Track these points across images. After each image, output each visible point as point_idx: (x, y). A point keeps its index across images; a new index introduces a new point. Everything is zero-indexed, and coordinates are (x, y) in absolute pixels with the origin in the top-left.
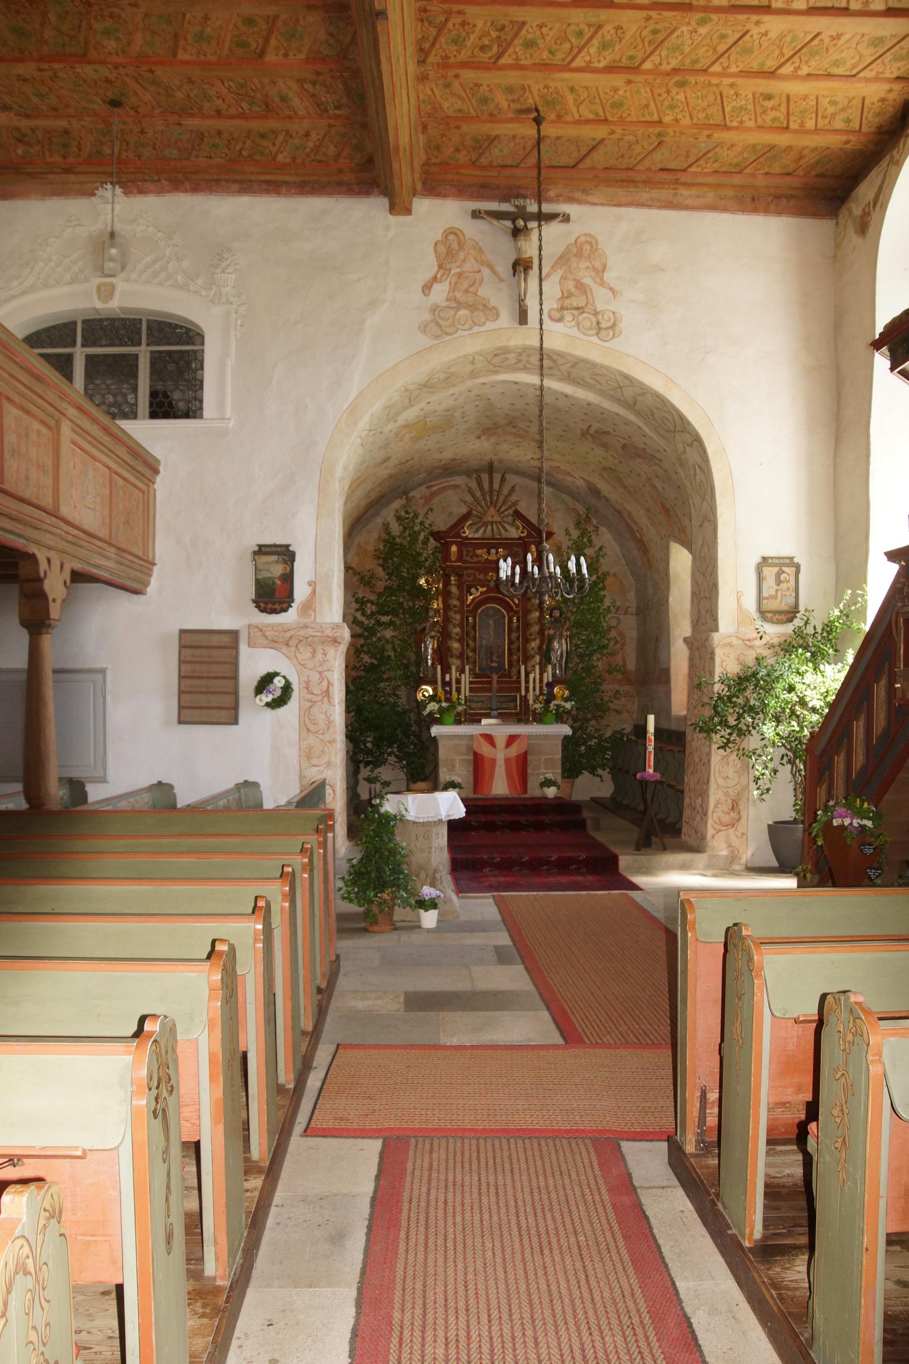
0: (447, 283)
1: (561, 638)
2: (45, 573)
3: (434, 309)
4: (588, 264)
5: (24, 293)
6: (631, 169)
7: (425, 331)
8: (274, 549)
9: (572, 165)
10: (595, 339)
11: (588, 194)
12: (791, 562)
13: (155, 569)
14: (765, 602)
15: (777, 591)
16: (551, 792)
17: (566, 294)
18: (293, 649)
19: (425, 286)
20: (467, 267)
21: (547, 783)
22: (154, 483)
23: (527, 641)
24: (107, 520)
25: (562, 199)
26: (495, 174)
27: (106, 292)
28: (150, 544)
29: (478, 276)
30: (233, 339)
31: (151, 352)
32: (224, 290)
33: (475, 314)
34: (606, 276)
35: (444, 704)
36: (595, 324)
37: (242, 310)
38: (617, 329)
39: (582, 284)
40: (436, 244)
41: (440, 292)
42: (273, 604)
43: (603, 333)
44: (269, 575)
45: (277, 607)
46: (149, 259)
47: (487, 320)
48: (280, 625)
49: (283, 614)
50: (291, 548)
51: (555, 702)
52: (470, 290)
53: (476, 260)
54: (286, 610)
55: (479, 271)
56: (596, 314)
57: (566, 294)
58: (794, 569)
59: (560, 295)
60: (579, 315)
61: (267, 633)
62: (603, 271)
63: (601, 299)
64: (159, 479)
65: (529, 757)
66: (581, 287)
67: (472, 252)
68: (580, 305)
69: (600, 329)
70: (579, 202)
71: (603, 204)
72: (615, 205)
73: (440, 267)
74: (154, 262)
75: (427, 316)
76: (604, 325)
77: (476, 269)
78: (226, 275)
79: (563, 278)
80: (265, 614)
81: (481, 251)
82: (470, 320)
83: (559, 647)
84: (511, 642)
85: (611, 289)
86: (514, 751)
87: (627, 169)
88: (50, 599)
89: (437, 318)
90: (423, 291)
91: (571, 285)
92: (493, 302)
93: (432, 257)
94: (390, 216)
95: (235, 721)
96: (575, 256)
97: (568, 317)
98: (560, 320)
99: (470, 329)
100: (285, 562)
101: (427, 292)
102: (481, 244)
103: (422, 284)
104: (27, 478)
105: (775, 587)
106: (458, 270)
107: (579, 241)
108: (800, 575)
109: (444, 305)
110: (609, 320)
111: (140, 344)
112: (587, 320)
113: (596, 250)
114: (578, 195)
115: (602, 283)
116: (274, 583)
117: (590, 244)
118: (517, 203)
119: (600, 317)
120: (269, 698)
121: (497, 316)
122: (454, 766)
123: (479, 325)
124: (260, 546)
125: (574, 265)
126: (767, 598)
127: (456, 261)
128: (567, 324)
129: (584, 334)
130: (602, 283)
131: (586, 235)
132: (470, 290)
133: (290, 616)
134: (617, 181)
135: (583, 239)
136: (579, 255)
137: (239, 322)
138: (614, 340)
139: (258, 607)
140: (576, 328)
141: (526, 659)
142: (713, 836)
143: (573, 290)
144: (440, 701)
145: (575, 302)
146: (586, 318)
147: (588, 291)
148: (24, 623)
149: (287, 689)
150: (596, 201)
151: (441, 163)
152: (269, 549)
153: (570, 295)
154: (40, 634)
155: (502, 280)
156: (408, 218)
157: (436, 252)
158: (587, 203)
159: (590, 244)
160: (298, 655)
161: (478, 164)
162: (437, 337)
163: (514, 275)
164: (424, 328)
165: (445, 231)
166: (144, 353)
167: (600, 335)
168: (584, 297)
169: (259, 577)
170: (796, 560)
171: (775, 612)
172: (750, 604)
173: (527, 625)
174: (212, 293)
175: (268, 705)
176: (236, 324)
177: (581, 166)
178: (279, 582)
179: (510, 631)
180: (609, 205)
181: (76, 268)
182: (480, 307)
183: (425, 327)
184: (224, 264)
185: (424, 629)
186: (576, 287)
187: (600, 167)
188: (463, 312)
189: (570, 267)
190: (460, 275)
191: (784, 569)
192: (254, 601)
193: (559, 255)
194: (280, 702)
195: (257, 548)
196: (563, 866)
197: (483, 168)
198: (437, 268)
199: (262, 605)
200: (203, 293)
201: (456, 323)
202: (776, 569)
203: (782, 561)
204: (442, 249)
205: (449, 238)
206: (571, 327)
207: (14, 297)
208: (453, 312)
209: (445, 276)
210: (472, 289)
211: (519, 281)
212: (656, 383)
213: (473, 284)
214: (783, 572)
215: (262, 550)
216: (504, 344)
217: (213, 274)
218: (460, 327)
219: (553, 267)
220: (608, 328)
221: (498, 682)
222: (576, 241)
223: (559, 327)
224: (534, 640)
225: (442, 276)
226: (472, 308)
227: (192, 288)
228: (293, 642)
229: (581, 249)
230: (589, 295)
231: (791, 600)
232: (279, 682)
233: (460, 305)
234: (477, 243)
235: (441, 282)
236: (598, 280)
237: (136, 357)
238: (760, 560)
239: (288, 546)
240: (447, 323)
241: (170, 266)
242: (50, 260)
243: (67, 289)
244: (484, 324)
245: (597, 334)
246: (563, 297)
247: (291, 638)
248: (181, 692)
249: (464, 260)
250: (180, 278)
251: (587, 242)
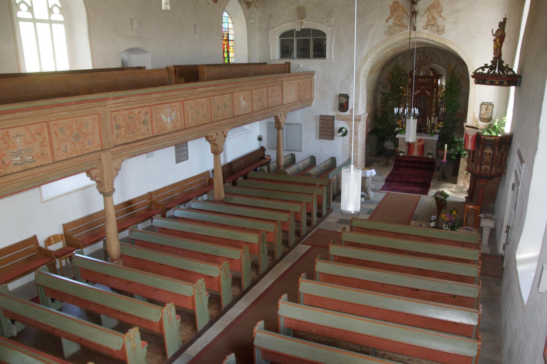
0: (393, 19)
1: (442, 108)
2: (280, 118)
3: (389, 27)
4: (436, 10)
5: (281, 24)
7: (386, 34)
8: (344, 95)
10: (437, 34)
12: (491, 104)
13: (314, 99)
14: (482, 115)
15: (486, 112)
16: (430, 156)
17: (429, 20)
18: (348, 121)
20: (399, 13)
21: (429, 154)
22: (313, 77)
23: (431, 108)
24: (298, 95)
27: (302, 24)
28: (312, 93)
30: (334, 37)
31: (314, 39)
32: (331, 23)
34: (442, 14)
35: (401, 129)
37: (336, 28)
38: (444, 31)
40: (390, 7)
41: (391, 21)
42: (343, 109)
43: (440, 32)
44: (342, 102)
45: (344, 110)
46: (312, 14)
47: (404, 29)
48: (345, 115)
49: (346, 112)
50: (348, 95)
51: (434, 130)
53: (402, 11)
54: (346, 111)
56: (438, 26)
58: (492, 106)
59: (427, 21)
61: (342, 117)
63: (440, 22)
64: (315, 75)
65: (425, 145)
66: (434, 18)
67: (401, 9)
68: (433, 24)
74: (313, 15)
75: (387, 29)
76: (440, 30)
78: (332, 19)
79: (428, 15)
80: (341, 112)
81: (404, 8)
83: (442, 109)
84: (427, 108)
85: (443, 18)
86: (420, 144)
88: (281, 123)
90: (386, 22)
91: (430, 17)
93: (389, 10)
95: (333, 139)
96: (433, 8)
97: (429, 28)
98: (426, 29)
99: (399, 33)
100: (347, 99)
101: (387, 21)
103: (386, 19)
104: (274, 101)
105: (485, 111)
106: (397, 14)
108: (494, 108)
109: (392, 25)
110: (442, 28)
111: (310, 37)
112: (435, 28)
113: (439, 6)
115: (441, 16)
116: (344, 104)
117: (438, 4)
119: (439, 27)
120: (341, 134)
122: (403, 146)
123: (402, 31)
124: (340, 94)
126: (482, 115)
128: (429, 30)
129: (433, 33)
130: (441, 16)
133: (348, 113)
135: (435, 2)
136: (434, 8)
137: (335, 32)
138: (443, 35)
139: (339, 110)
140: (431, 31)
141: (431, 113)
142: (459, 180)
143: (431, 19)
144: (400, 127)
145: (431, 23)
146: (434, 28)
148: (276, 128)
149: (346, 132)
152: (342, 95)
153: (430, 21)
154: (279, 130)
159: (438, 4)
160: (350, 123)
162: (389, 35)
164: (386, 33)
165: (393, 2)
166: (311, 39)
169: (340, 102)
170: (493, 104)
171: (484, 119)
172: (477, 116)
173: (432, 103)
174: (328, 24)
175: (341, 135)
176: (334, 33)
178: (345, 104)
179: (427, 104)
181: (293, 17)
182: (403, 26)
184: (331, 15)
185: (400, 103)
188: (398, 27)
190: (397, 16)
191: (489, 106)
192: (338, 109)
194: (344, 135)
195: (339, 95)
196: (415, 184)
198: (390, 14)
199: (340, 110)
200: (326, 24)
202: (486, 106)
203: (488, 104)
204: (392, 8)
207: (278, 26)
208: (394, 28)
210: (400, 20)
212: (454, 48)
214: (488, 107)
215: (341, 95)
217: (328, 18)
218: (396, 32)
219: (425, 12)
220: (441, 31)
221: (421, 120)
222: (433, 3)
223: (426, 31)
224: (434, 108)
225: (392, 16)
226: (400, 26)
227: (323, 22)
228: (348, 120)
230: (436, 20)
231: (490, 116)
232: (344, 130)
233: (396, 25)
234: (403, 6)
236: (439, 15)
237: (310, 39)
238: (481, 103)
239: (347, 95)
241: (317, 16)
242: (286, 15)
243: (291, 23)
244: (403, 31)
245: (437, 33)
246: (428, 22)
247: (347, 119)
248: (320, 131)
249: (399, 11)
250: (320, 20)
251: (437, 3)
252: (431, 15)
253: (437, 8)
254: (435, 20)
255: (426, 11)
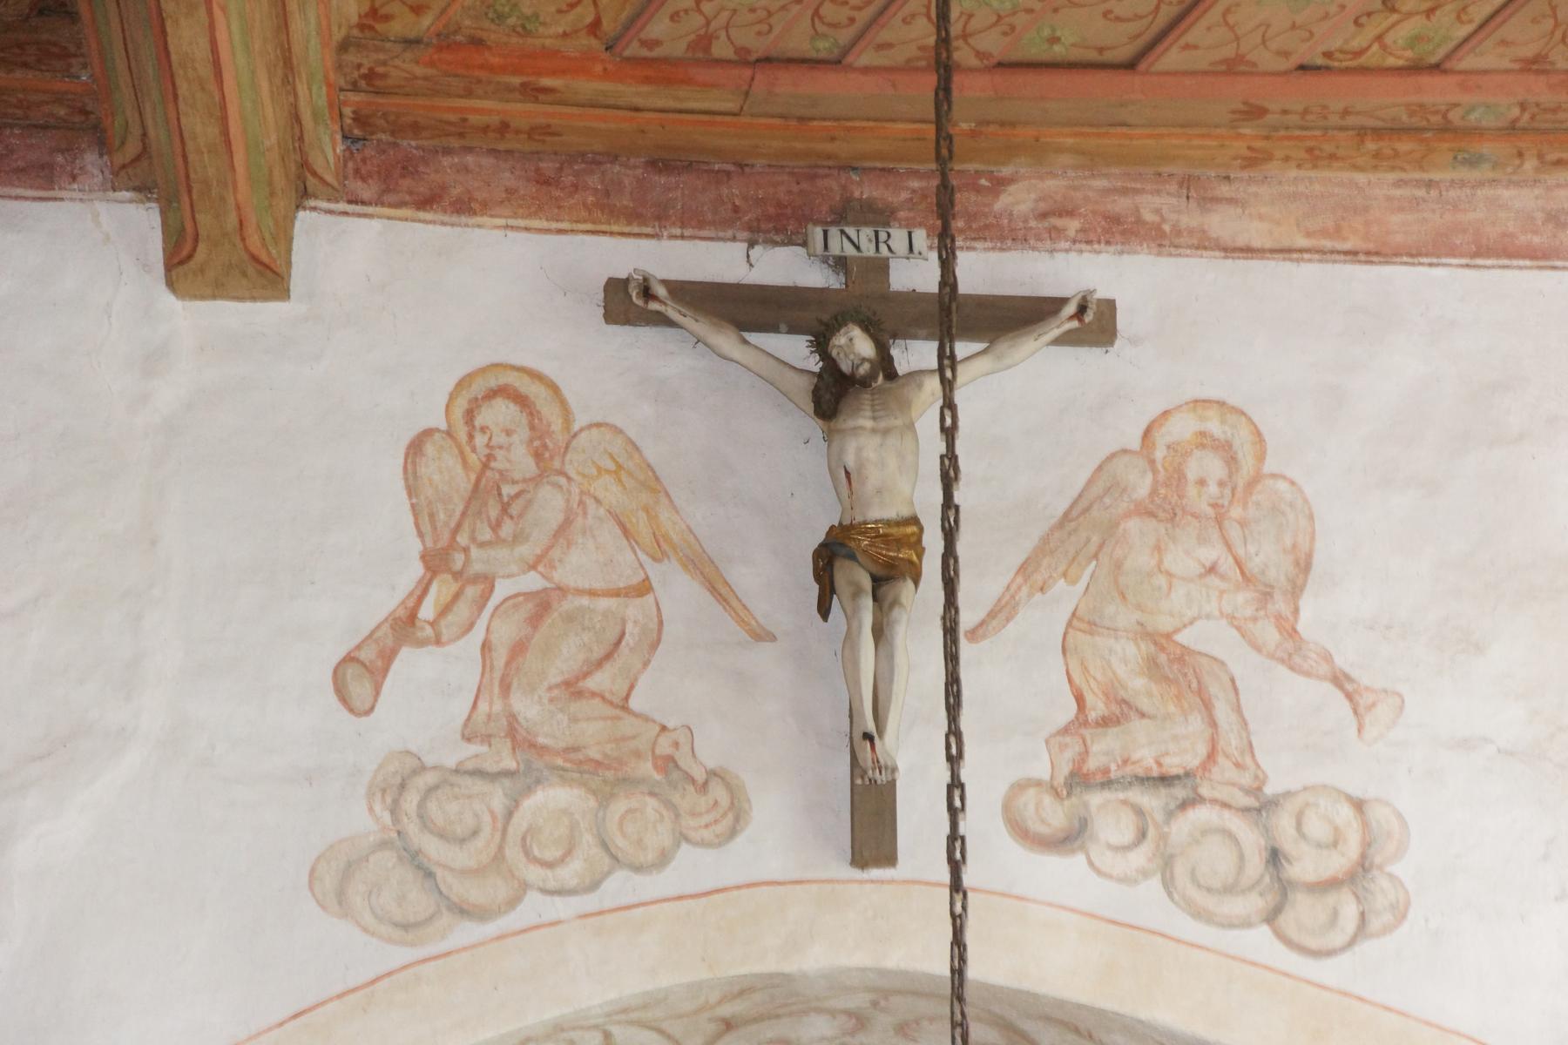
6: (1437, 68)
9: (1124, 53)
10: (1260, 941)
11: (1208, 202)
17: (1097, 707)
19: (349, 659)
25: (1073, 225)
26: (725, 101)
29: (635, 610)
33: (619, 807)
34: (1311, 615)
36: (1256, 864)
38: (1382, 892)
39: (1184, 656)
40: (416, 447)
43: (1304, 912)
47: (682, 837)
52: (591, 683)
55: (644, 588)
56: (1262, 807)
57: (1097, 707)
59: (1067, 710)
60: (1170, 815)
62: (1295, 590)
67: (610, 491)
68: (1173, 765)
69: (1284, 889)
70: (1161, 239)
71: (1285, 252)
72: (1352, 255)
73: (435, 562)
76: (1306, 866)
77: (636, 579)
81: (652, 483)
82: (588, 839)
85: (1340, 680)
87: (1416, 68)
89: (412, 828)
92: (713, 746)
94: (168, 300)
98: (1070, 839)
99: (594, 886)
101: (360, 690)
102: (651, 452)
106: (532, 582)
107: (1162, 439)
109: (459, 753)
114: (1155, 204)
117: (1226, 450)
118: (838, 245)
119: (1284, 823)
121: (736, 816)
123: (638, 869)
125: (1140, 559)
127: (518, 538)
128: (1106, 860)
129: (1200, 914)
131: (1199, 404)
132: (591, 683)
134: (1362, 133)
135: (1182, 428)
138: (1366, 947)
140: (1155, 883)
143: (1137, 685)
146: (1206, 831)
147: (1214, 689)
150: (1255, 233)
151: (445, 41)
153: (1120, 712)
155: (761, 635)
156: (265, 314)
157: (411, 491)
158: (1204, 244)
159: (1226, 450)
161: (633, 49)
163: (824, 610)
167: (1287, 920)
168: (1196, 723)
177: (1172, 58)
180: (1323, 254)
182: (646, 768)
183: (347, 873)
186: (1152, 667)
187: (1267, 60)
189: (1118, 565)
190: (541, 605)
193: (1061, 506)
197: (661, 71)
198: (417, 570)
201: (513, 853)
205: (485, 417)
206: (1124, 880)
209: (462, 611)
210: (599, 681)
211: (850, 640)
213: (608, 656)
216: (770, 965)
218: (534, 874)
219: (1023, 569)
220: (1330, 885)
222: (1147, 433)
225: (445, 611)
229: (1177, 477)
230: (1222, 712)
235: (438, 641)
236: (1269, 634)
240: (461, 857)
244: (664, 859)
245: (1272, 917)
251: (1204, 440)
252: (1125, 618)
253: (1219, 521)
254: (1207, 706)
255: (1044, 548)
